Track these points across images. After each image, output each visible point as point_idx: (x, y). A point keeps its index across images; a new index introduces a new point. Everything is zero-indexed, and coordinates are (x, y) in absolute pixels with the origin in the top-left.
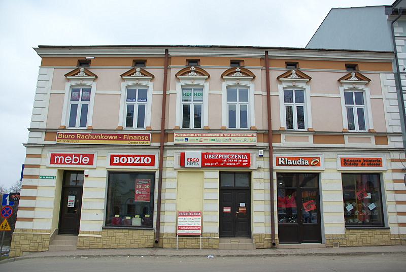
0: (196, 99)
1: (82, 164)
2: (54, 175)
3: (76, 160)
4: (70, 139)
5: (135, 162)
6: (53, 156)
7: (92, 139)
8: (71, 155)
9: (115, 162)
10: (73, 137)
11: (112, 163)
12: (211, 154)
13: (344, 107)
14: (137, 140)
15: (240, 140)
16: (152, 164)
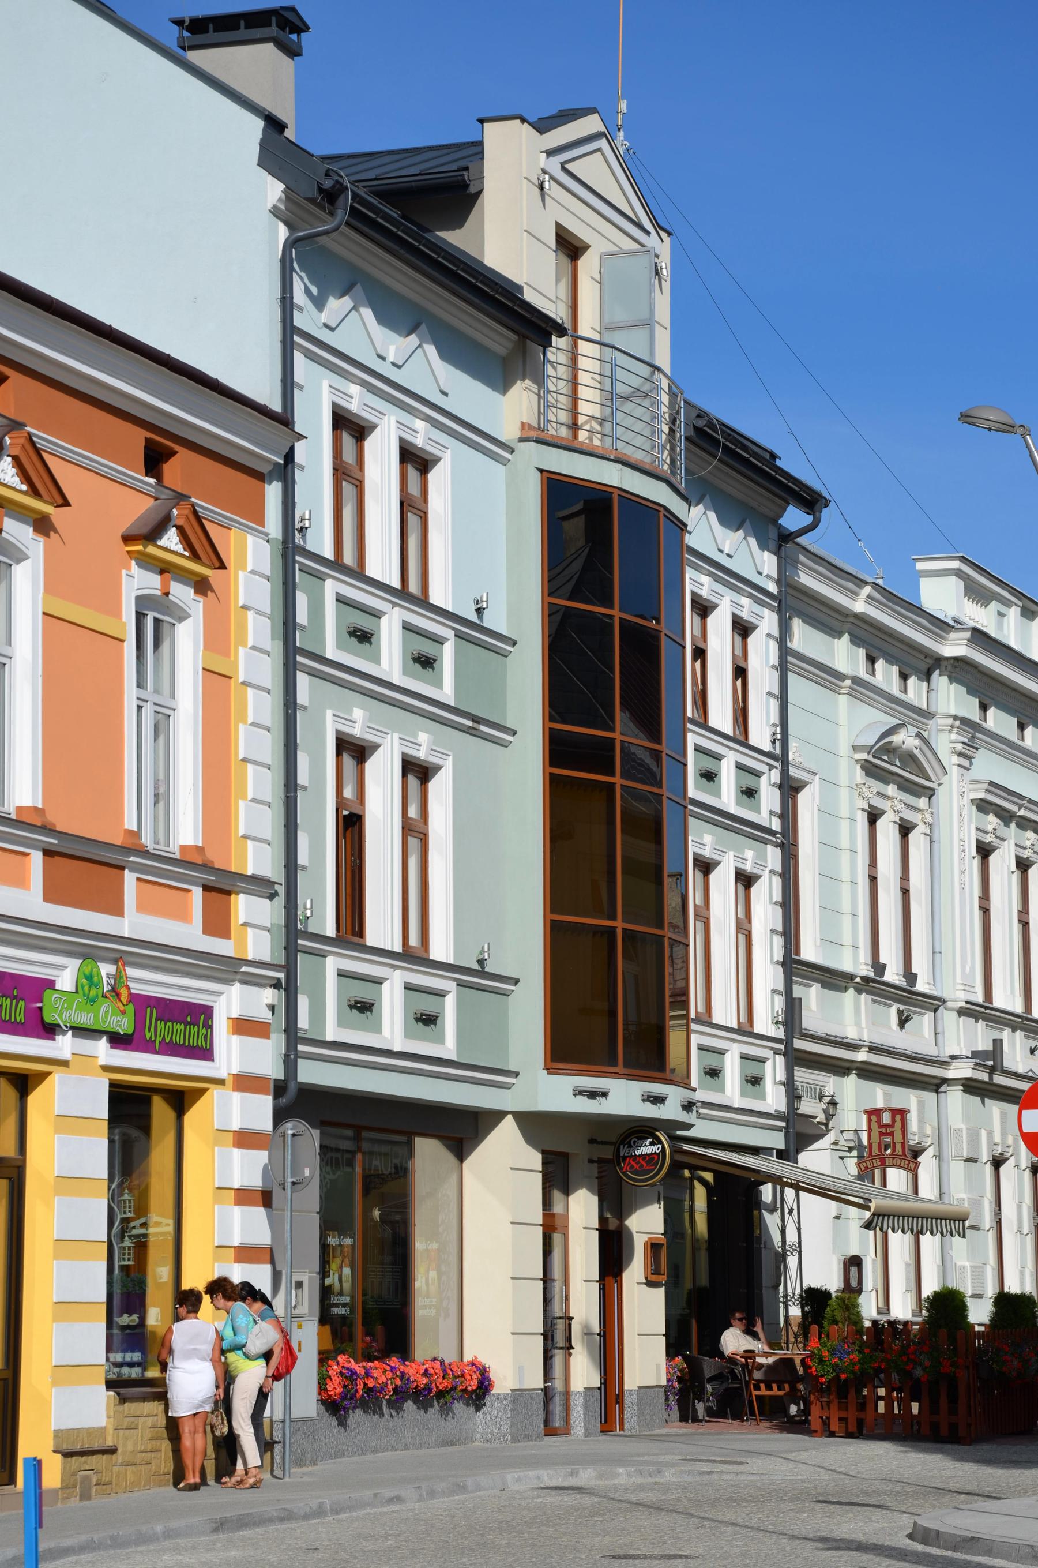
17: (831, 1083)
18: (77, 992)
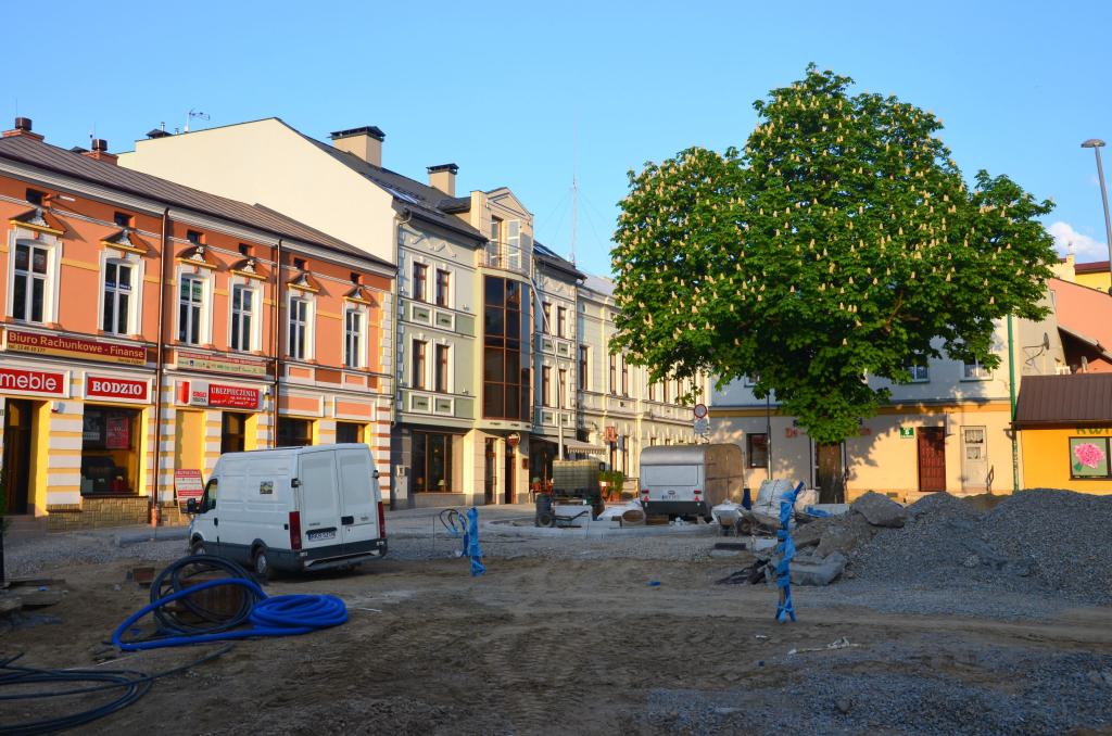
1: (46, 390)
3: (35, 383)
4: (30, 343)
5: (122, 392)
7: (65, 349)
8: (27, 374)
9: (94, 390)
11: (90, 391)
12: (219, 387)
15: (249, 370)
16: (143, 396)
17: (595, 420)
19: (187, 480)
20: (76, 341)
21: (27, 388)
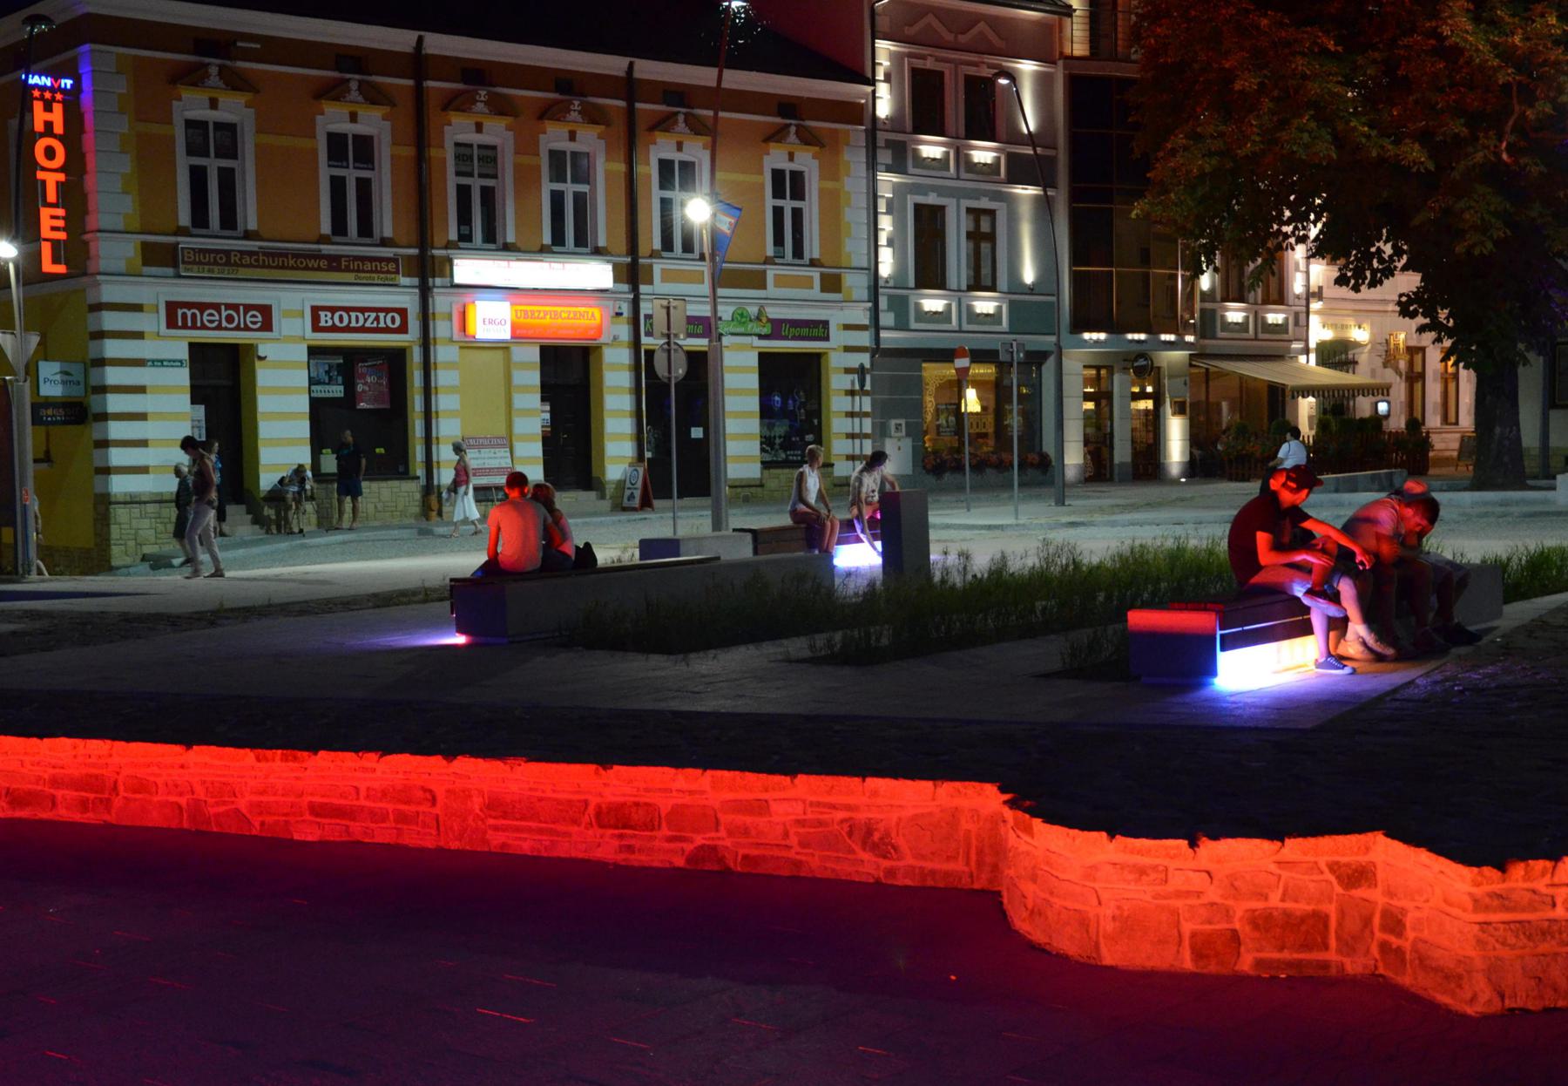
0: (485, 171)
1: (247, 329)
2: (179, 358)
3: (230, 319)
4: (216, 263)
5: (368, 324)
6: (172, 307)
7: (269, 267)
8: (216, 307)
9: (322, 324)
10: (221, 258)
11: (316, 328)
13: (770, 202)
14: (371, 271)
18: (733, 320)
19: (485, 452)
20: (286, 255)
21: (219, 328)
